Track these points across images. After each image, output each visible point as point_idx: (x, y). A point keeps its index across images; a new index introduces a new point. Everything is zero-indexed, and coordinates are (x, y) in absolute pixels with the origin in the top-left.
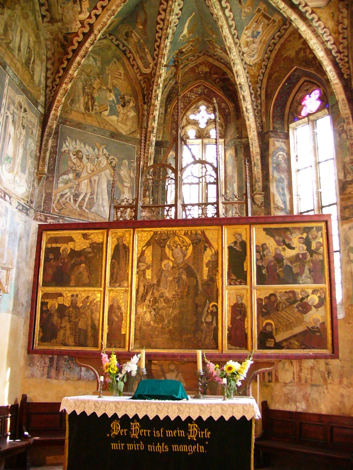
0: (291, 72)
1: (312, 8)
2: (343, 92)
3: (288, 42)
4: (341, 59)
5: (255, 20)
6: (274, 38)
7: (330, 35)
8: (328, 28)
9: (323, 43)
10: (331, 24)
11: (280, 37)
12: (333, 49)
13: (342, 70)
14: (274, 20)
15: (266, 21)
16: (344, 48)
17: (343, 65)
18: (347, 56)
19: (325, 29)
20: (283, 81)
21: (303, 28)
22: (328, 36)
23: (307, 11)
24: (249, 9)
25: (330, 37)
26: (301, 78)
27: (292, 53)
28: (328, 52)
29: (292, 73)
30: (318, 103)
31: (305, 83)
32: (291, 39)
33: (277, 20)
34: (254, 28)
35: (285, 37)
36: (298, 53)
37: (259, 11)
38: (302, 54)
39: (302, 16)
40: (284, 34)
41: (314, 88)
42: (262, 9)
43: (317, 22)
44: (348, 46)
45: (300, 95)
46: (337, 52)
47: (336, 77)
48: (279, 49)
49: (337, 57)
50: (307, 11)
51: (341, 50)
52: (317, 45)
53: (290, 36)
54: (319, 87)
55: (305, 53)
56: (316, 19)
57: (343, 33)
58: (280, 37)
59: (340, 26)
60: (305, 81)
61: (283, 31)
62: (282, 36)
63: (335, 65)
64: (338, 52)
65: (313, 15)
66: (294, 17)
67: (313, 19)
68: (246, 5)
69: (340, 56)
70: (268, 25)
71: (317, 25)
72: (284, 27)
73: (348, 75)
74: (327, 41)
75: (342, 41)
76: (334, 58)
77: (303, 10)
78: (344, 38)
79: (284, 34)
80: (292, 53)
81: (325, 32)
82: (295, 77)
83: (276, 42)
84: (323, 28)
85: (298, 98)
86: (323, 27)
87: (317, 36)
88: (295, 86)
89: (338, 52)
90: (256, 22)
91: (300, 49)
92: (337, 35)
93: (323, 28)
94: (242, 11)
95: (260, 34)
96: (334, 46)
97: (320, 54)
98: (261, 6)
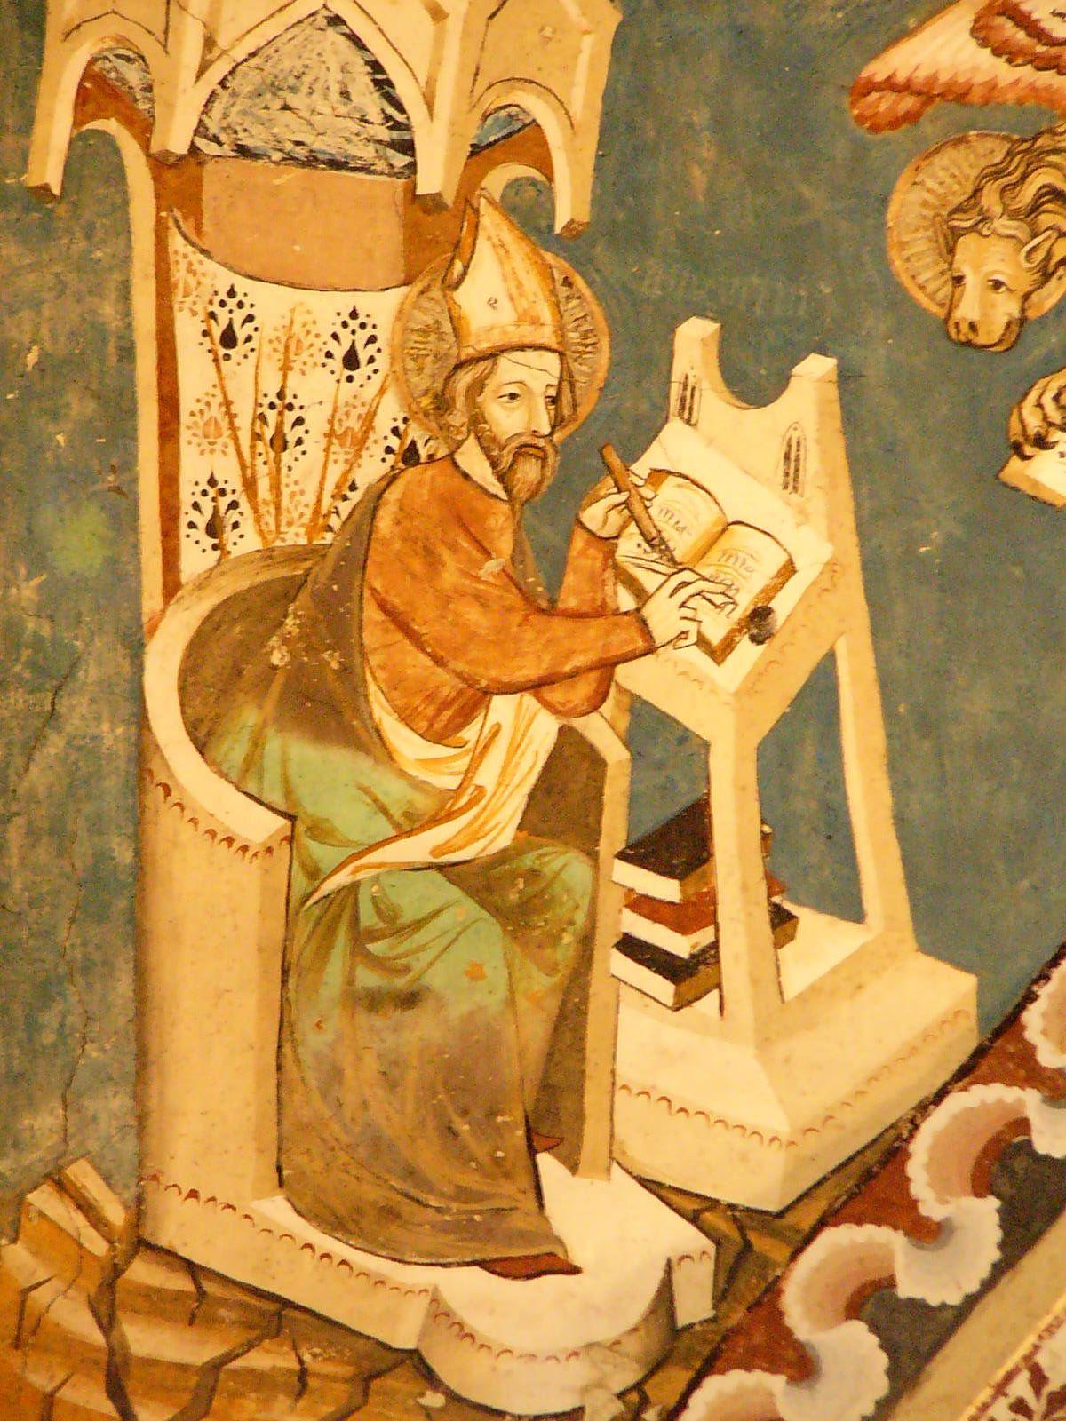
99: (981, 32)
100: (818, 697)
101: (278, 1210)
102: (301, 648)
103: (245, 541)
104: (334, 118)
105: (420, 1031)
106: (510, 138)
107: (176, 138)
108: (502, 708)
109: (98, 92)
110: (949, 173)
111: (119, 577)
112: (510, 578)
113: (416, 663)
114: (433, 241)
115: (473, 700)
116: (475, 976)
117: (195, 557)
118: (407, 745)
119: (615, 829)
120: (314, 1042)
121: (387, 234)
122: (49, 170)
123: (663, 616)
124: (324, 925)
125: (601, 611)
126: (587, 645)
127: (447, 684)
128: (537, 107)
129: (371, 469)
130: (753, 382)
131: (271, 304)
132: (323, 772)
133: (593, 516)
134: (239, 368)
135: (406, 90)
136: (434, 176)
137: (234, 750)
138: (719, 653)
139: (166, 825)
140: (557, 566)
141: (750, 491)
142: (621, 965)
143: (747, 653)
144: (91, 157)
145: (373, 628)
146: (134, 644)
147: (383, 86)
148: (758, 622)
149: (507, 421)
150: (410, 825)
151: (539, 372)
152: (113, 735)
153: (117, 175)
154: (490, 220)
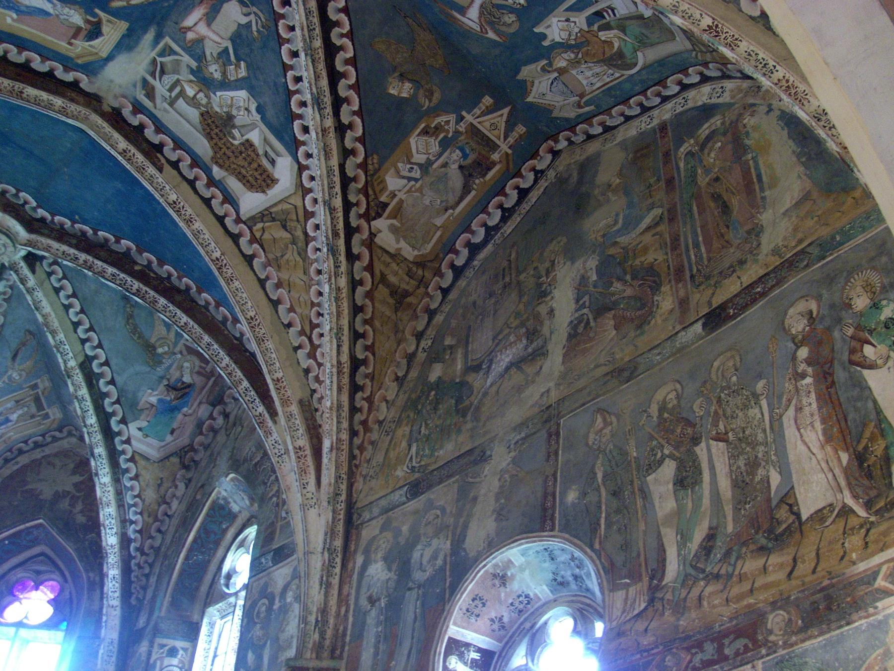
0: (28, 525)
1: (134, 452)
2: (118, 627)
3: (49, 463)
4: (139, 566)
5: (17, 398)
6: (26, 442)
7: (141, 513)
8: (143, 501)
9: (124, 522)
10: (151, 495)
11: (37, 445)
12: (135, 540)
13: (133, 585)
14: (47, 414)
15: (34, 410)
16: (152, 547)
17: (137, 577)
18: (151, 566)
19: (137, 499)
20: (7, 534)
21: (104, 479)
22: (136, 513)
23: (123, 452)
24: (20, 375)
25: (139, 516)
26: (39, 544)
27: (47, 492)
28: (125, 541)
29: (27, 528)
30: (49, 611)
31: (41, 558)
32: (57, 462)
33: (52, 418)
34: (6, 409)
35: (47, 451)
36: (58, 496)
37: (35, 387)
38: (65, 504)
39: (113, 456)
40: (47, 444)
41: (53, 576)
42: (41, 386)
43: (131, 479)
44: (159, 548)
45: (20, 574)
46: (137, 549)
47: (117, 594)
48: (25, 467)
49: (134, 558)
50: (123, 452)
51: (146, 550)
52: (113, 521)
53: (56, 455)
54: (66, 581)
55: (72, 505)
56: (132, 474)
57: (162, 522)
58: (37, 445)
59: (164, 507)
60: (42, 554)
61: (49, 439)
62: (42, 446)
63: (126, 570)
64: (140, 549)
65: (131, 465)
66: (100, 450)
67: (127, 470)
68: (21, 367)
69: (139, 559)
70: (33, 416)
71: (128, 484)
72: (57, 434)
73: (137, 598)
74: (132, 522)
75: (153, 534)
76: (131, 557)
77: (120, 448)
78: (159, 531)
79: (47, 444)
80: (47, 492)
81: (135, 505)
82: (30, 537)
83: (26, 448)
84: (135, 497)
85: (13, 577)
86: (136, 493)
87: (121, 505)
88: (20, 552)
89: (140, 549)
90: (17, 402)
91: (66, 494)
92: (151, 520)
93: (135, 497)
94: (6, 372)
95: (10, 424)
96: (138, 535)
97: (111, 539)
98: (43, 381)
99: (487, 33)
100: (568, 9)
101: (677, 38)
102: (617, 60)
103: (610, 71)
104: (561, 86)
105: (644, 31)
106: (543, 69)
107: (577, 98)
108: (603, 39)
109: (580, 107)
110: (503, 29)
111: (626, 80)
112: (588, 45)
113: (607, 49)
114: (562, 71)
115: (605, 42)
116: (634, 28)
117: (617, 75)
118: (616, 45)
119: (604, 21)
120: (657, 41)
121: (565, 75)
122: (592, 107)
123: (577, 30)
124: (643, 43)
125: (582, 36)
126: (588, 36)
127: (606, 46)
128: (539, 69)
129: (590, 65)
130: (544, 36)
131: (585, 82)
132: (628, 52)
133: (573, 42)
134: (593, 82)
135: (550, 81)
136: (556, 75)
137: (634, 60)
138: (575, 22)
139: (648, 62)
140: (582, 43)
141: (555, 28)
142: (617, 15)
143: (572, 19)
144: (587, 104)
145: (608, 55)
146: (632, 75)
147: (552, 83)
148: (568, 20)
149: (573, 56)
150: (624, 40)
151: (565, 56)
152: (644, 72)
153: (587, 101)
154: (554, 67)
